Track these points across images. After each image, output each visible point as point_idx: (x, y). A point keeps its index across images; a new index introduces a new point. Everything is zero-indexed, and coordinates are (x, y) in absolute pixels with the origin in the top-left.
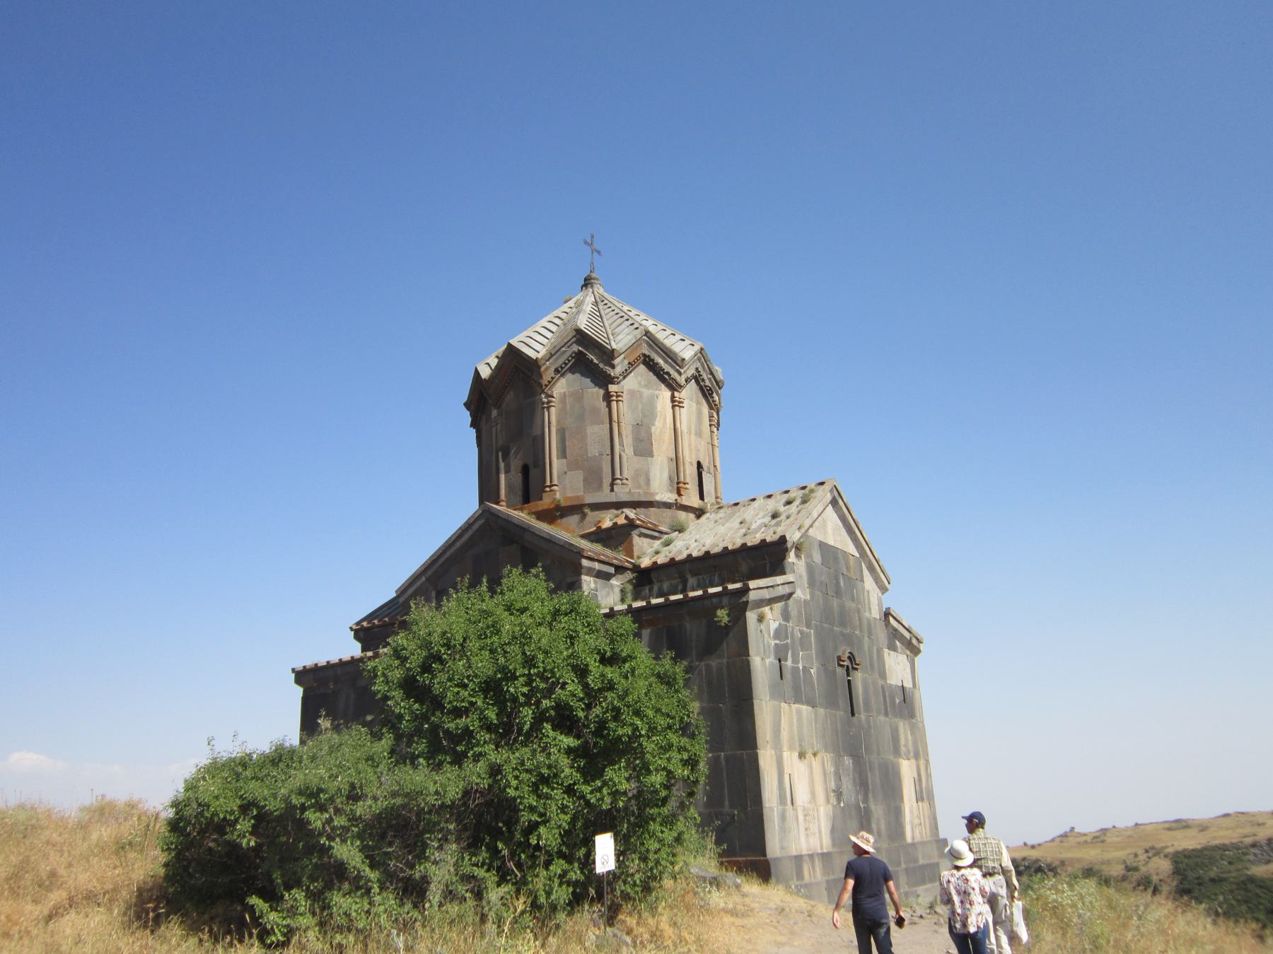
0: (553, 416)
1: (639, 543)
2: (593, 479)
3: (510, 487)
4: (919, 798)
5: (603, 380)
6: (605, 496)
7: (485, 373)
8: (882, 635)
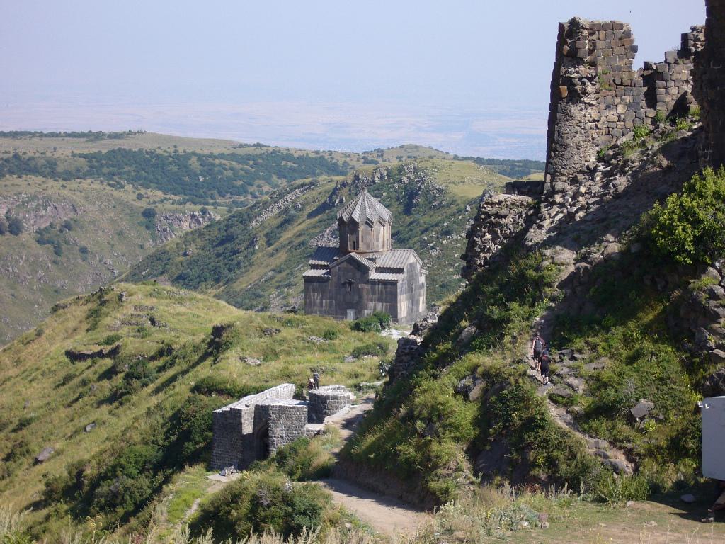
0: (361, 234)
1: (377, 261)
2: (368, 247)
3: (351, 245)
4: (423, 303)
5: (372, 227)
6: (371, 251)
7: (345, 219)
8: (419, 275)
